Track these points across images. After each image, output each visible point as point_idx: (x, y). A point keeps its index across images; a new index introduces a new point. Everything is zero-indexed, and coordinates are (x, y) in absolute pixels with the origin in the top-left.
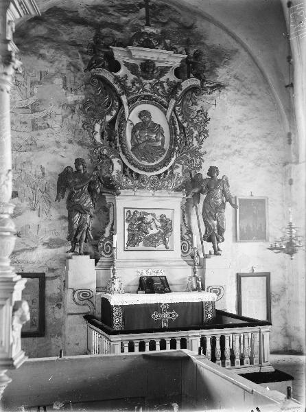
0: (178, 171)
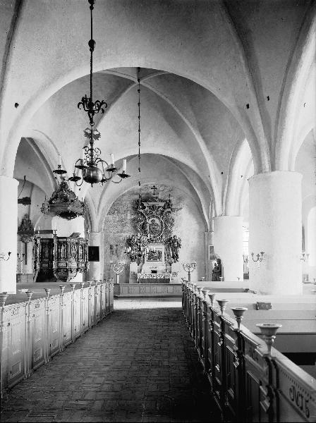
0: (164, 237)
